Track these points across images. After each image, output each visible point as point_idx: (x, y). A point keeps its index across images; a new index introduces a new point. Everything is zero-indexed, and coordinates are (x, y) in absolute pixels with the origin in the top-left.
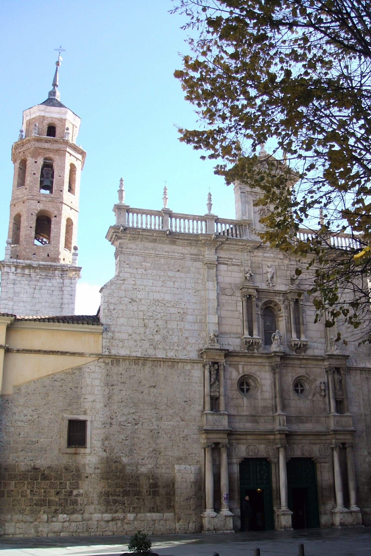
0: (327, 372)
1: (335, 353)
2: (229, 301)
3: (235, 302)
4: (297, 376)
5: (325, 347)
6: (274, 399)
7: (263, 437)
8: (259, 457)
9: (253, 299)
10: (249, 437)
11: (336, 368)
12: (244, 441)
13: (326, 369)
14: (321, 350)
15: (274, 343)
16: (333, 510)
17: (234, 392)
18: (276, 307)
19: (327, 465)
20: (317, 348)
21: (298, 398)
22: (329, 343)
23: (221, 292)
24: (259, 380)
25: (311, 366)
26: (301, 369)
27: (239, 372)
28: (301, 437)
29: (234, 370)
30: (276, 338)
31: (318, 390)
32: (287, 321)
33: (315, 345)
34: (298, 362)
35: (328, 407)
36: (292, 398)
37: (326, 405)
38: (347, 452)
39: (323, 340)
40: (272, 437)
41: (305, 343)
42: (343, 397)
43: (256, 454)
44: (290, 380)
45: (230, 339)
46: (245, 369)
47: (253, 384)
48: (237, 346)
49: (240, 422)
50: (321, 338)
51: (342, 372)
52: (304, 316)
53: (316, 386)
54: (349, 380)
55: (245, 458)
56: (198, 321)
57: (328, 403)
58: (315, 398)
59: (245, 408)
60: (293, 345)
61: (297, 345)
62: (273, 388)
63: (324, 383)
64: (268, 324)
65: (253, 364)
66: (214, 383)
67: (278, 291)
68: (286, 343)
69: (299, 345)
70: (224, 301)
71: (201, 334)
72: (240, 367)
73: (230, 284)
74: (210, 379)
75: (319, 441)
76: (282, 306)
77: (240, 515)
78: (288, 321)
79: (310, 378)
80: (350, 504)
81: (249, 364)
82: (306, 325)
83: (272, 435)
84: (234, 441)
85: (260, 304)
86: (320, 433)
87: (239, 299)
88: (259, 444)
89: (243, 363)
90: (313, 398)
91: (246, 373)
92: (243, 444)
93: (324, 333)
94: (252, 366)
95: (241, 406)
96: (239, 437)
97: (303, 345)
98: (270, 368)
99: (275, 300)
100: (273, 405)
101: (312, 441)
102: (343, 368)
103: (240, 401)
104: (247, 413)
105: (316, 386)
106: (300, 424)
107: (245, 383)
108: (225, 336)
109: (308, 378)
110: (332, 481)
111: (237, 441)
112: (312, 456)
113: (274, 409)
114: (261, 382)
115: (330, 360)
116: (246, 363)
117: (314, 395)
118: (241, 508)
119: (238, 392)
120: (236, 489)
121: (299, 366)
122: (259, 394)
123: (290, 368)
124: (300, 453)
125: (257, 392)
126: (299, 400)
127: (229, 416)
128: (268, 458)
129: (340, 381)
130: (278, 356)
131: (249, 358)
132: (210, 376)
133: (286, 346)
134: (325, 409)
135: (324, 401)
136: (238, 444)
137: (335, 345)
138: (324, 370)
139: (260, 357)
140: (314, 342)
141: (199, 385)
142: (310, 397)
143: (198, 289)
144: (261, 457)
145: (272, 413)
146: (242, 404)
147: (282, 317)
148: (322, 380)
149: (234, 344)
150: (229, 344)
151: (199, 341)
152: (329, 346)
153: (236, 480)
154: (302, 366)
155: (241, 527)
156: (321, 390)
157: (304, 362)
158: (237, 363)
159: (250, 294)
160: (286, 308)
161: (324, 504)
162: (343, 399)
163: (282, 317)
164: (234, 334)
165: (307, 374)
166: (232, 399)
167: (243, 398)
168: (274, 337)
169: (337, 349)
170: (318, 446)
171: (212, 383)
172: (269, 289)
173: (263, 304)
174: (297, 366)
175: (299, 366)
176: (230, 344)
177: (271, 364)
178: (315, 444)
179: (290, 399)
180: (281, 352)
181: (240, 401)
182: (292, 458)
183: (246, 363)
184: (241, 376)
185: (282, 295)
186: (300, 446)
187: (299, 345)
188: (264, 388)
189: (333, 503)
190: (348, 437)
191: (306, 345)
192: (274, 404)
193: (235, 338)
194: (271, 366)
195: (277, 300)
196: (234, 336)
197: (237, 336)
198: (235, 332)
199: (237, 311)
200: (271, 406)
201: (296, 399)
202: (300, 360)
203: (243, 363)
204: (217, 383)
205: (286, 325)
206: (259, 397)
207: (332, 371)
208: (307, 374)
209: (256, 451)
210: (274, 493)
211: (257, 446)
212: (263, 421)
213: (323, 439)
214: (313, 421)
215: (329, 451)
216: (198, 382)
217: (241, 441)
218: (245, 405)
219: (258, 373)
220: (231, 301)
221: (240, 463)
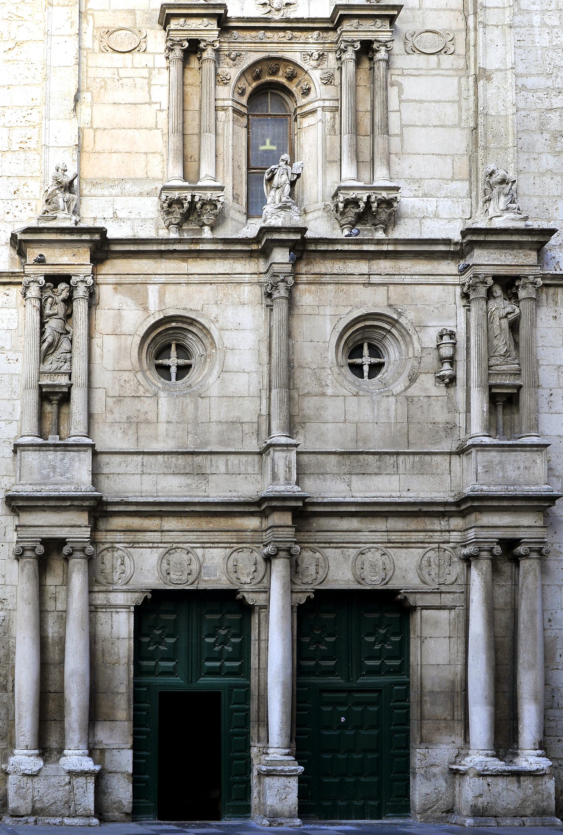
0: (465, 296)
1: (498, 223)
2: (123, 73)
3: (145, 73)
4: (357, 313)
5: (468, 210)
6: (264, 394)
7: (223, 523)
8: (202, 586)
9: (205, 55)
10: (170, 523)
11: (497, 278)
12: (156, 536)
13: (463, 285)
14: (450, 220)
15: (269, 200)
16: (454, 763)
17: (126, 376)
18: (296, 81)
19: (444, 614)
20: (436, 216)
21: (354, 390)
22: (481, 192)
23: (97, 43)
24: (215, 333)
25: (408, 280)
26: (370, 288)
27: (146, 309)
28: (354, 523)
29: (130, 302)
30: (277, 180)
31: (430, 360)
32: (328, 125)
33: (430, 205)
34: (362, 267)
35: (463, 416)
36: (329, 391)
37: (456, 411)
38: (521, 572)
39: (462, 187)
40: (253, 523)
41: (384, 194)
42: (518, 382)
43: (192, 578)
44: (329, 328)
45: (120, 202)
46: (170, 299)
47: (196, 348)
48: (144, 220)
49: (143, 473)
50: (452, 180)
51: (522, 294)
52: (393, 103)
53: (423, 349)
54: (552, 322)
55: (155, 592)
56: (15, 147)
57: (462, 407)
58: (414, 391)
59: (162, 428)
60: (341, 205)
61: (355, 202)
62: (265, 358)
63: (452, 335)
64: (268, 146)
65: (196, 278)
66: (53, 346)
67: (298, 20)
68: (321, 205)
69: (362, 205)
70: (108, 74)
71: (23, 190)
72: (153, 292)
73: (132, 12)
74: (42, 333)
75: (421, 536)
76: (316, 75)
77: (131, 770)
78: (333, 126)
79: (403, 321)
80: (518, 749)
81: (184, 279)
82: (401, 135)
83: (252, 514)
84: (119, 537)
85: (234, 73)
86: (425, 509)
87: (162, 62)
88: (204, 545)
89: (163, 279)
90: (406, 388)
91: (171, 313)
92: (152, 545)
93: (466, 159)
94: (194, 288)
95: (147, 422)
96: (136, 522)
97: (381, 202)
98: (258, 291)
99: (288, 55)
100: (260, 416)
101: (394, 537)
102: (526, 277)
103: (147, 405)
104: (170, 446)
105: (423, 349)
106: (354, 478)
107: (173, 347)
108: (106, 192)
109: (394, 322)
110: (459, 668)
111: (130, 537)
112: (390, 586)
113: (264, 428)
114: (221, 338)
115: (477, 252)
116: (171, 279)
117: (412, 379)
118: (136, 747)
119: (140, 376)
120: (123, 689)
121: (364, 279)
122: (212, 379)
123: (330, 287)
124: (349, 576)
125: (209, 374)
126: (357, 395)
127: (95, 454)
128: (235, 592)
129: (514, 326)
130: (282, 243)
131: (184, 260)
132: (42, 325)
133: (320, 213)
134: (450, 428)
135: (450, 398)
136: (133, 544)
137: (499, 194)
138: (458, 290)
139: (224, 254)
140: (425, 195)
141: (11, 355)
142: (398, 387)
143: (19, 39)
144: (209, 586)
145: (255, 442)
146: (151, 416)
147: (313, 112)
148: (450, 325)
149: (133, 216)
150: (115, 217)
151: (17, 213)
152: (481, 204)
153: (124, 661)
154: (375, 279)
155: (134, 807)
156: (442, 360)
157: (384, 265)
158: (140, 279)
159: (193, 35)
160: (328, 81)
161: (426, 742)
162: (519, 387)
163: (313, 112)
164: (136, 180)
165: (390, 306)
166: (120, 399)
167: (156, 395)
168: (270, 180)
169: (507, 209)
170: (417, 553)
171: (45, 345)
172: (269, 16)
173: (243, 73)
174: (355, 279)
175: (364, 279)
176: (120, 215)
177: (263, 278)
178: (405, 545)
179: (323, 394)
180: (289, 230)
181: (147, 405)
182: (317, 592)
183: (171, 279)
184: (152, 321)
185: (316, 33)
186: (352, 552)
187: (362, 205)
188: (232, 361)
189: (459, 741)
190: (527, 520)
191: (389, 203)
192: (264, 411)
193: (141, 194)
194: (260, 284)
195: (297, 57)
196: (137, 190)
197: (147, 188)
198: (141, 174)
199: (150, 103)
200: (255, 420)
201: (346, 393)
202: (369, 260)
203: (163, 279)
204: (65, 345)
205: (324, 140)
206: (214, 391)
207: (482, 291)
208: (390, 306)
209: (195, 567)
210: (254, 706)
211: (199, 552)
212: (222, 469)
213: (438, 528)
214: (401, 466)
215: (458, 568)
216: (8, 347)
217: (140, 536)
218: (163, 417)
219: (213, 311)
220: (130, 72)
221: (136, 607)
